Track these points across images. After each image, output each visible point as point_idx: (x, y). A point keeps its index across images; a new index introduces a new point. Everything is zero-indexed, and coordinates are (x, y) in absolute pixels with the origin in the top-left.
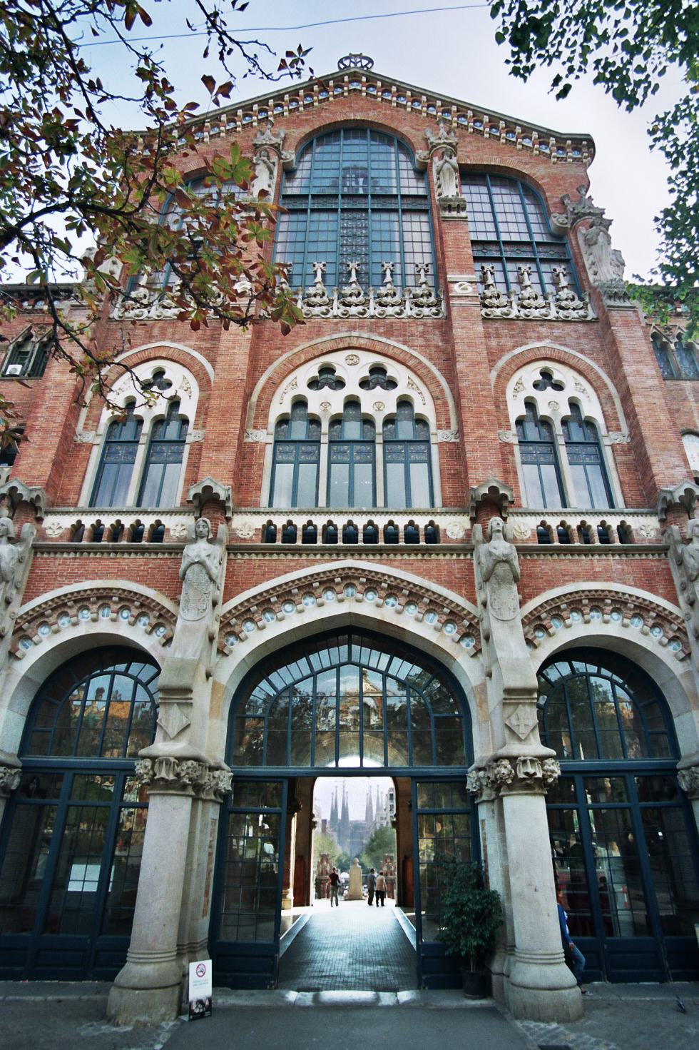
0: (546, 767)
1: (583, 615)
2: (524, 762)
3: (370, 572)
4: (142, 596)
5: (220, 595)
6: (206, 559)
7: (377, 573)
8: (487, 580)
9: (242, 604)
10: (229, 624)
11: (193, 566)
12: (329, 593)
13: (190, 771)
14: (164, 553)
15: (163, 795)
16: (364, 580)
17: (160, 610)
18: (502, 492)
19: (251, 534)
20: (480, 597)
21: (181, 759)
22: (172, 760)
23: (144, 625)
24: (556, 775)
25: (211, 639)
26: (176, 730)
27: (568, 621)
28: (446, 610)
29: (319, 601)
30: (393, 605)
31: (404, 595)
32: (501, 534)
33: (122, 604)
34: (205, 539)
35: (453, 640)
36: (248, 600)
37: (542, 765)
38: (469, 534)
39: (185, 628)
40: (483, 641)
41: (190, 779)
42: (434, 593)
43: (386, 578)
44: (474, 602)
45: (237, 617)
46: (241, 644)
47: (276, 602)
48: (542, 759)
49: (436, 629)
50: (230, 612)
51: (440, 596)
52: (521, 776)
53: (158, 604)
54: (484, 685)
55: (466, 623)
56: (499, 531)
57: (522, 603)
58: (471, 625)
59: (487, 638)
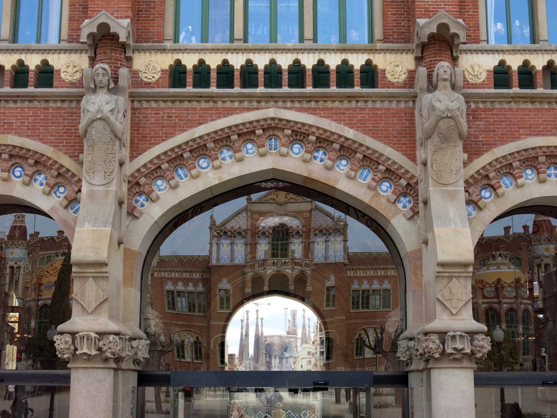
0: (476, 342)
1: (538, 173)
2: (453, 337)
3: (296, 123)
4: (36, 153)
5: (126, 153)
6: (109, 114)
7: (303, 124)
8: (421, 145)
9: (151, 161)
10: (138, 184)
11: (96, 124)
12: (249, 146)
13: (111, 345)
14: (55, 101)
15: (86, 368)
16: (289, 132)
17: (58, 169)
18: (453, 30)
19: (157, 77)
20: (420, 154)
21: (102, 335)
22: (93, 335)
23: (41, 184)
24: (485, 351)
25: (121, 203)
26: (94, 306)
27: (520, 181)
28: (381, 167)
29: (238, 155)
30: (322, 160)
31: (335, 150)
32: (448, 84)
33: (13, 161)
34: (105, 90)
35: (388, 201)
36: (158, 157)
37: (472, 341)
38: (412, 76)
39: (92, 195)
40: (421, 205)
41: (113, 354)
42: (368, 148)
43: (314, 130)
44: (413, 159)
45: (145, 176)
46: (154, 204)
47: (189, 158)
48: (472, 334)
49: (369, 187)
50: (139, 170)
51: (376, 152)
52: (449, 351)
53: (56, 162)
54: (420, 250)
55: (404, 182)
56: (445, 80)
57: (465, 164)
58: (408, 184)
59: (426, 203)
